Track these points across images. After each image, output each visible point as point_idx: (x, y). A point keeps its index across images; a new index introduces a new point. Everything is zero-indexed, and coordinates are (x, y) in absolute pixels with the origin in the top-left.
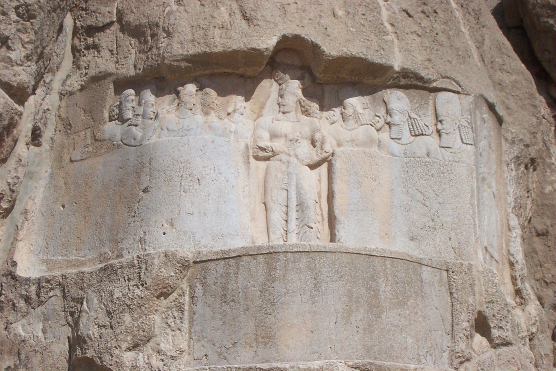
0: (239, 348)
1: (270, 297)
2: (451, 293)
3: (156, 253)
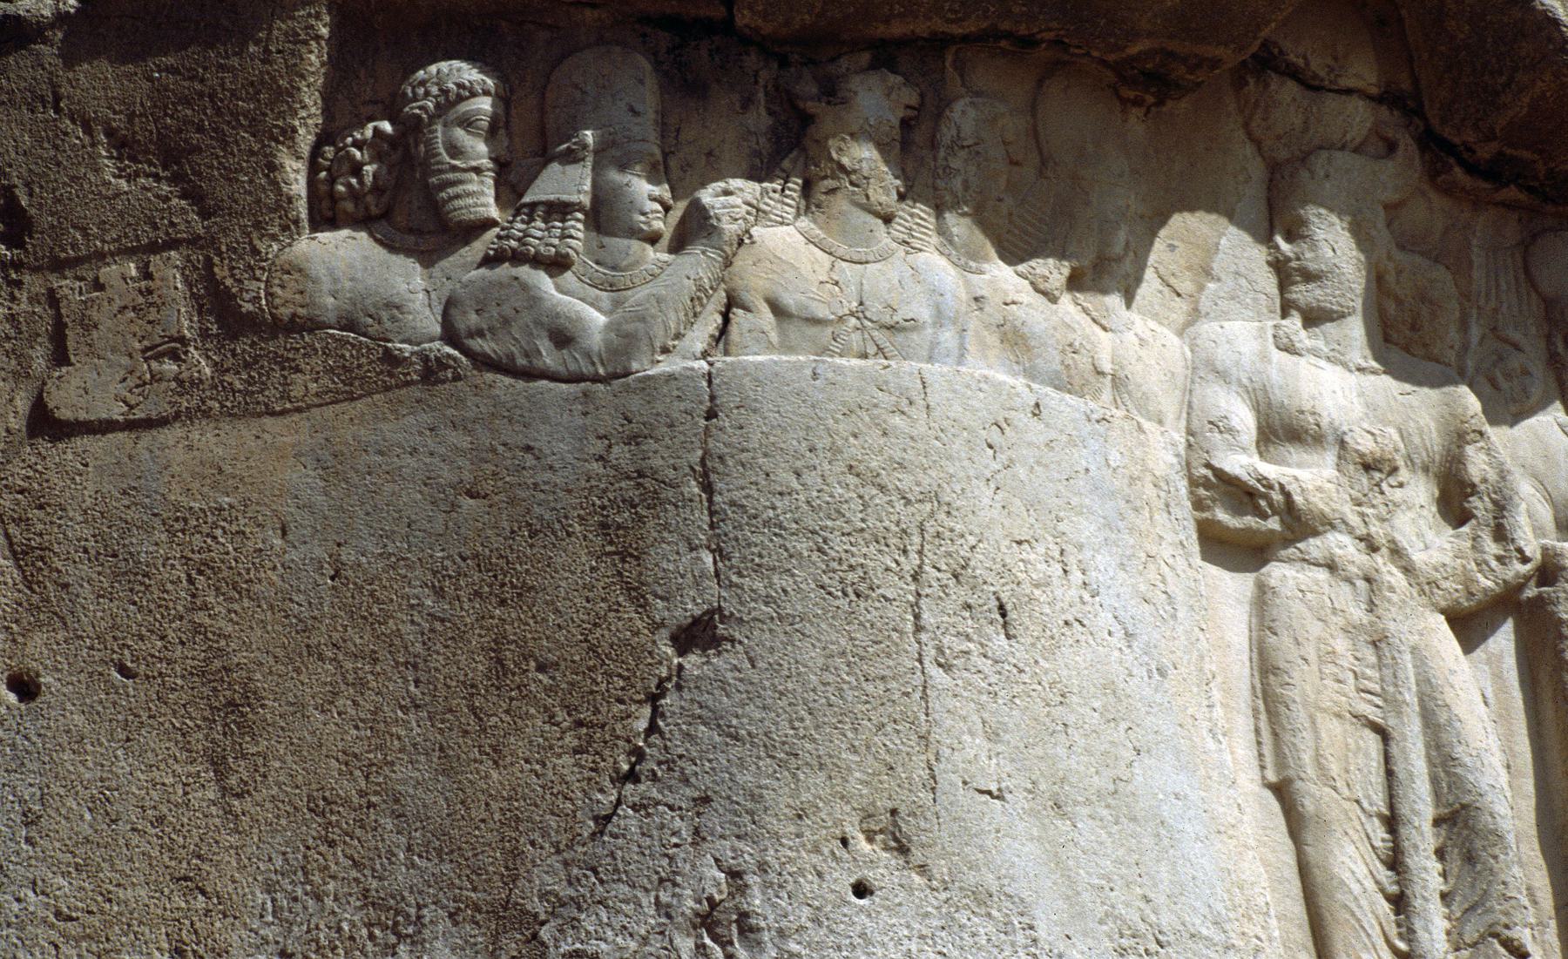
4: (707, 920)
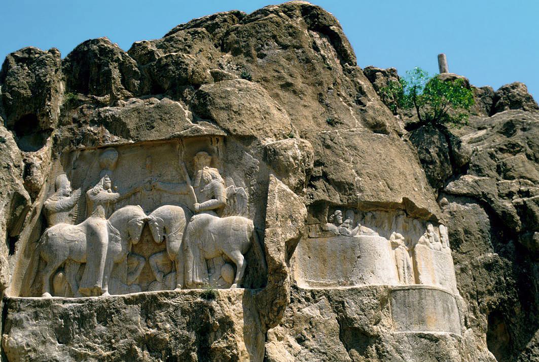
2: (458, 308)
4: (360, 279)
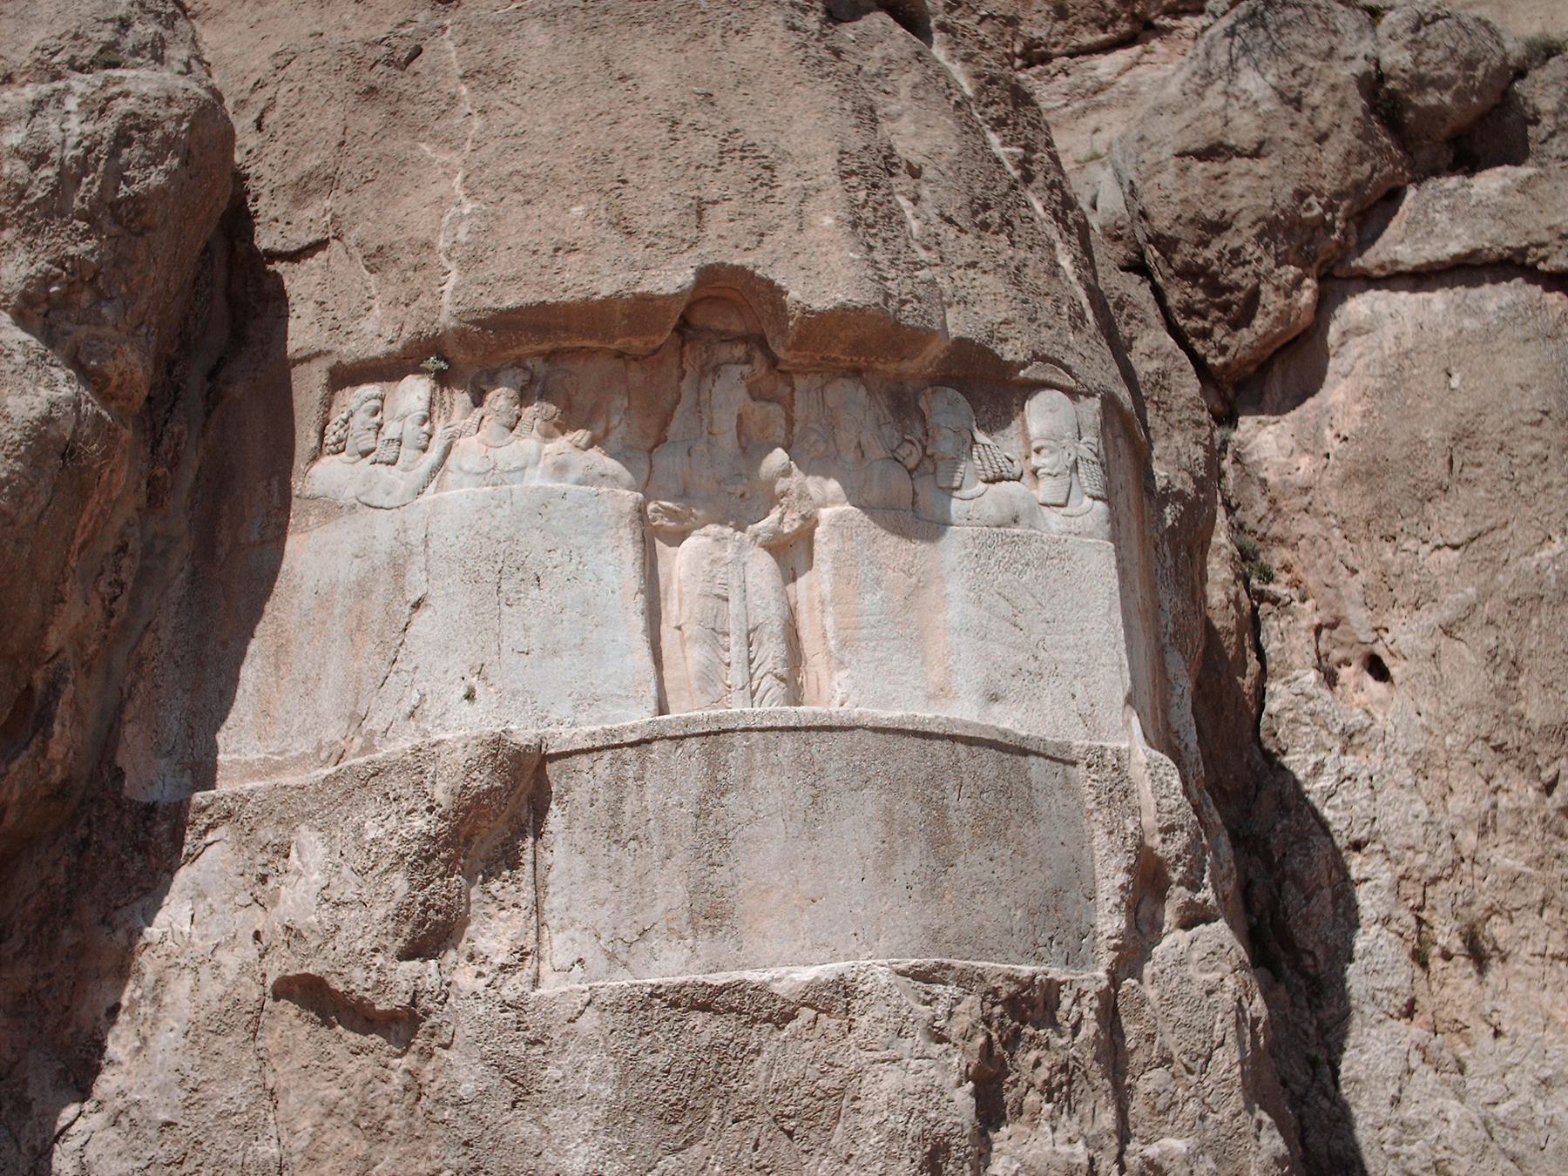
0: (655, 942)
1: (719, 827)
3: (459, 739)
